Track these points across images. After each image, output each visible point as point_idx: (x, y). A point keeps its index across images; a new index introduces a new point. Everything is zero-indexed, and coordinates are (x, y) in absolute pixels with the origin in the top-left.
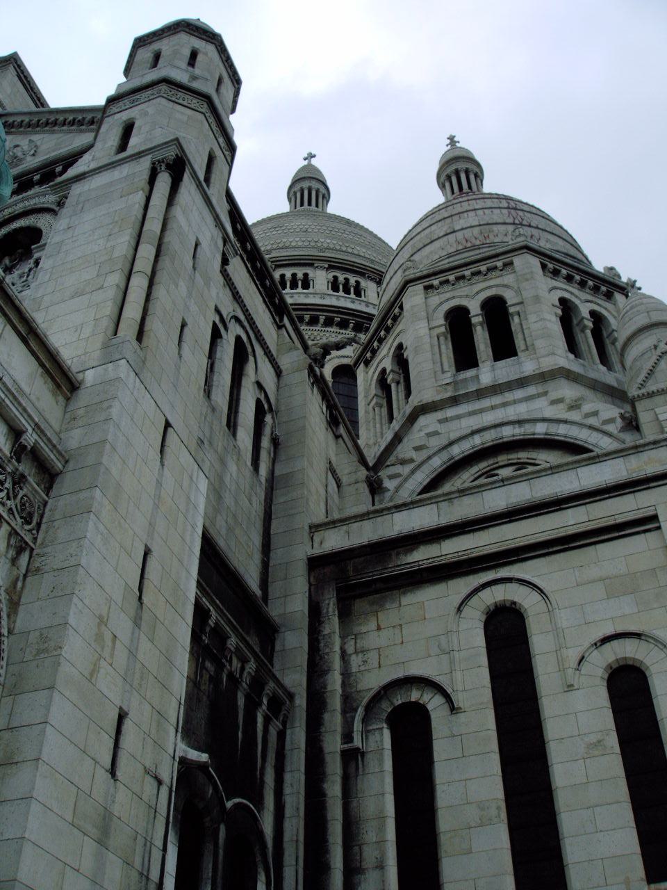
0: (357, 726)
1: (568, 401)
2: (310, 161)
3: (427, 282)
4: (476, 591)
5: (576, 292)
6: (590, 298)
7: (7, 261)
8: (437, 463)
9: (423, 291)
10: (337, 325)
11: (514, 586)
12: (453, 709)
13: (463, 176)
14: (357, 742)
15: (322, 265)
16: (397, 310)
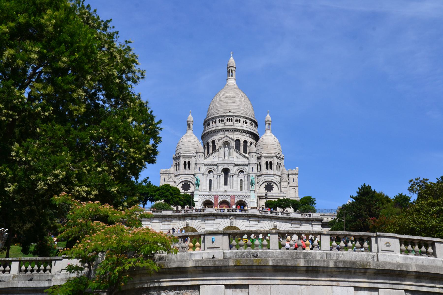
8: (263, 181)
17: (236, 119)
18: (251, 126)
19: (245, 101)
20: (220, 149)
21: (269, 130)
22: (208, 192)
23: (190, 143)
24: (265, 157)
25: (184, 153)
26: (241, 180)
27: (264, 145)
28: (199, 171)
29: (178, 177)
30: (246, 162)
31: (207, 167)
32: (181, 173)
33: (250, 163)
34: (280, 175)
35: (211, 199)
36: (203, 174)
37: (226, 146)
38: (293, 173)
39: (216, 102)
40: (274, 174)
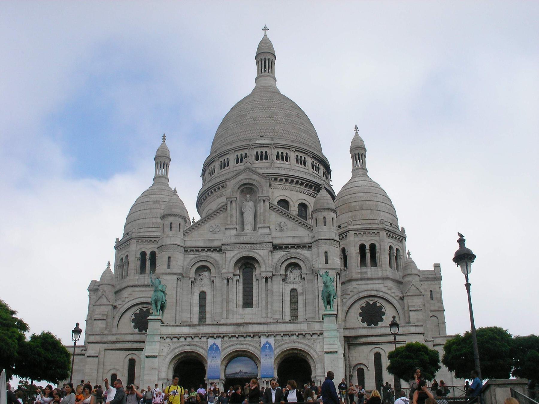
0: (352, 371)
1: (388, 287)
2: (265, 33)
3: (355, 232)
4: (373, 349)
5: (393, 241)
6: (395, 242)
7: (290, 269)
8: (356, 297)
9: (354, 236)
10: (300, 184)
11: (380, 349)
12: (368, 370)
13: (360, 157)
14: (352, 374)
15: (293, 150)
16: (344, 236)
17: (278, 153)
18: (315, 171)
20: (229, 205)
21: (362, 168)
22: (186, 325)
23: (160, 208)
25: (142, 230)
26: (293, 290)
27: (353, 204)
28: (169, 266)
29: (125, 293)
31: (192, 256)
32: (131, 283)
33: (316, 238)
34: (401, 280)
35: (198, 349)
37: (248, 196)
38: (428, 276)
40: (384, 276)
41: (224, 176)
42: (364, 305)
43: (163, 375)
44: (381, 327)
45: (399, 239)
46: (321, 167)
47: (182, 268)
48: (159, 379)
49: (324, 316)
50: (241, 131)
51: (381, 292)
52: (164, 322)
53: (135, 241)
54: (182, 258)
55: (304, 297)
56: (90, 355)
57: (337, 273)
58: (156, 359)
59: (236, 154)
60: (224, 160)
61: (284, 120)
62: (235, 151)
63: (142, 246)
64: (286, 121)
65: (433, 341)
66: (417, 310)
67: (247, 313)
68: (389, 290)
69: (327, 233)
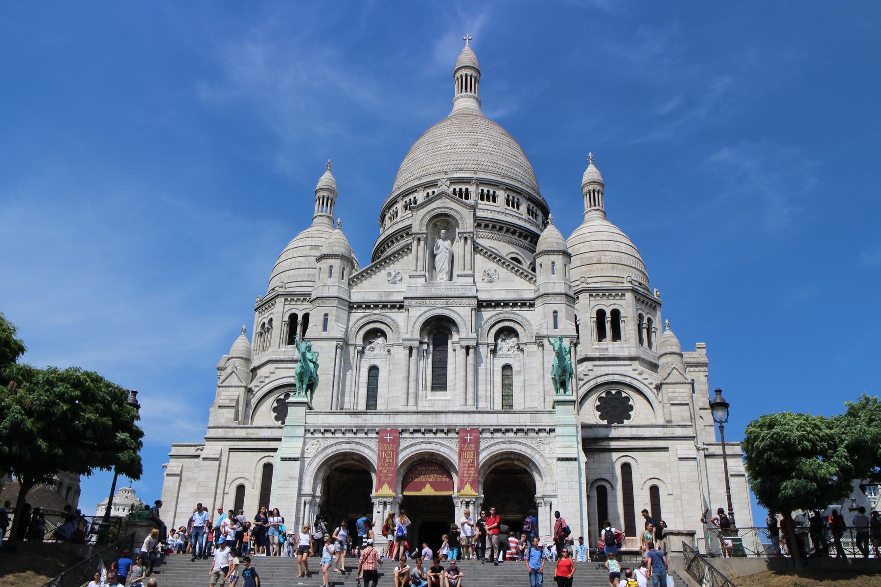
5: (643, 308)
8: (592, 384)
13: (596, 194)
17: (482, 190)
18: (531, 217)
19: (509, 146)
20: (415, 244)
21: (598, 210)
24: (593, 293)
26: (507, 367)
28: (325, 329)
30: (526, 291)
32: (274, 357)
33: (542, 292)
35: (362, 448)
36: (344, 344)
37: (443, 231)
38: (689, 360)
39: (419, 150)
41: (409, 220)
42: (604, 395)
43: (307, 488)
44: (631, 427)
45: (651, 304)
46: (539, 213)
47: (344, 330)
48: (300, 495)
49: (556, 404)
50: (433, 162)
51: (628, 378)
52: (314, 407)
53: (283, 299)
54: (346, 317)
55: (523, 375)
56: (207, 457)
57: (572, 342)
58: (298, 463)
59: (427, 192)
60: (410, 199)
61: (491, 149)
62: (424, 188)
63: (292, 306)
64: (494, 150)
65: (707, 449)
66: (681, 404)
67: (437, 398)
68: (639, 374)
69: (556, 284)
